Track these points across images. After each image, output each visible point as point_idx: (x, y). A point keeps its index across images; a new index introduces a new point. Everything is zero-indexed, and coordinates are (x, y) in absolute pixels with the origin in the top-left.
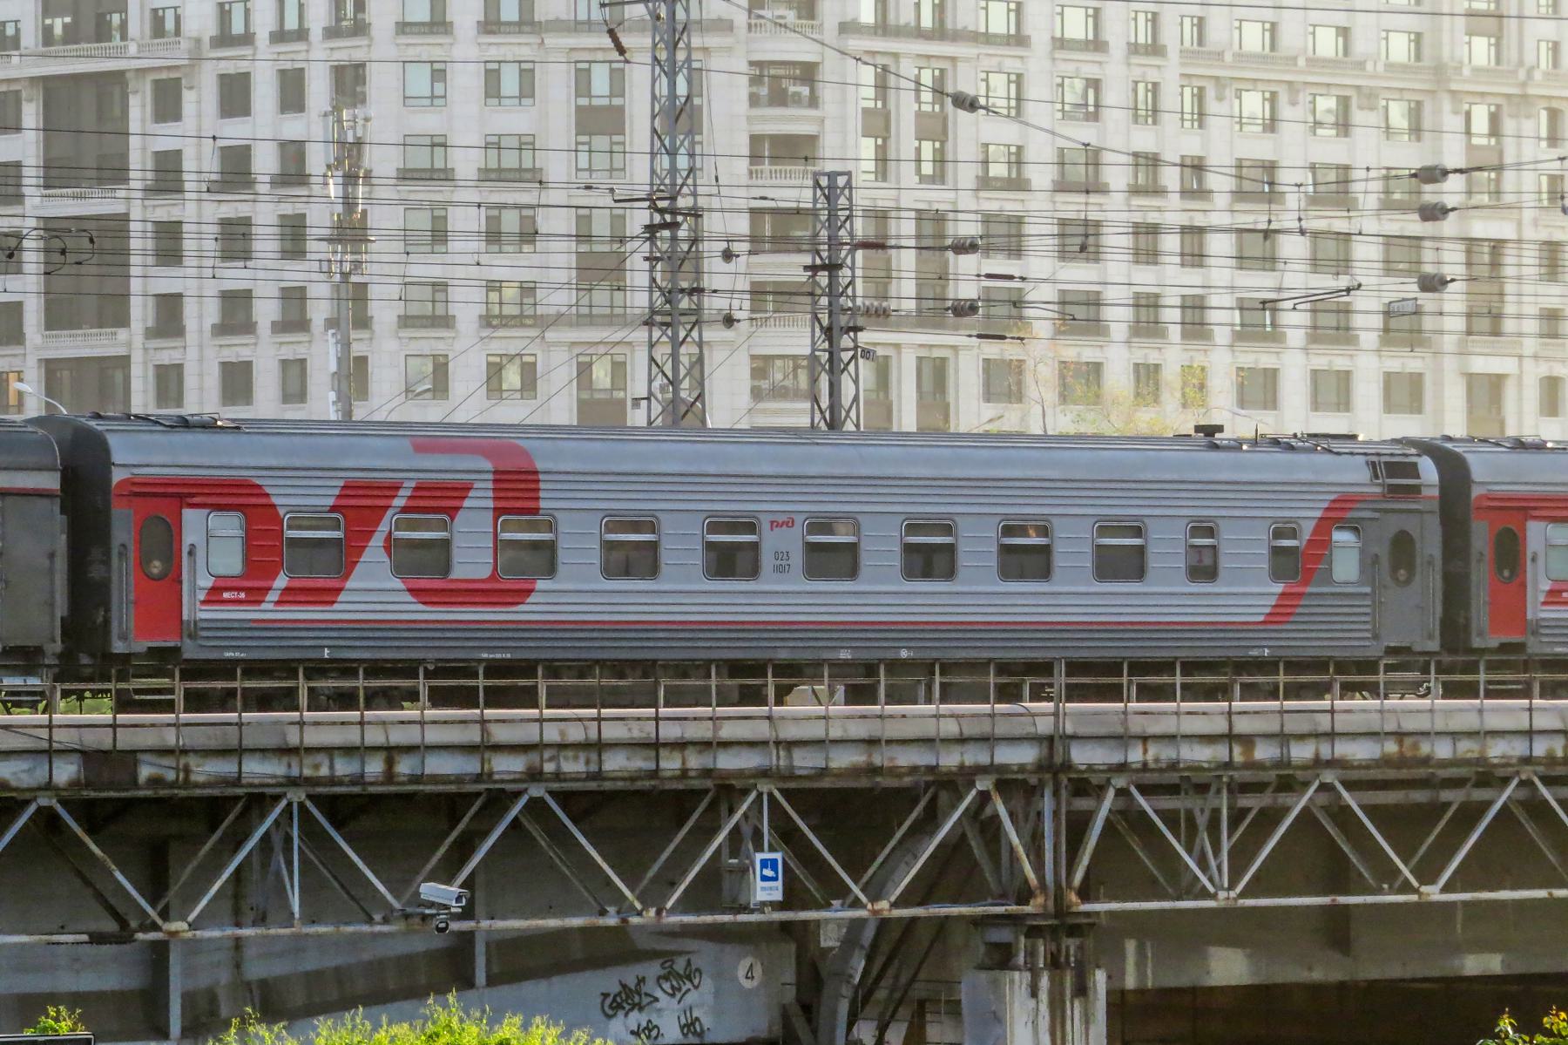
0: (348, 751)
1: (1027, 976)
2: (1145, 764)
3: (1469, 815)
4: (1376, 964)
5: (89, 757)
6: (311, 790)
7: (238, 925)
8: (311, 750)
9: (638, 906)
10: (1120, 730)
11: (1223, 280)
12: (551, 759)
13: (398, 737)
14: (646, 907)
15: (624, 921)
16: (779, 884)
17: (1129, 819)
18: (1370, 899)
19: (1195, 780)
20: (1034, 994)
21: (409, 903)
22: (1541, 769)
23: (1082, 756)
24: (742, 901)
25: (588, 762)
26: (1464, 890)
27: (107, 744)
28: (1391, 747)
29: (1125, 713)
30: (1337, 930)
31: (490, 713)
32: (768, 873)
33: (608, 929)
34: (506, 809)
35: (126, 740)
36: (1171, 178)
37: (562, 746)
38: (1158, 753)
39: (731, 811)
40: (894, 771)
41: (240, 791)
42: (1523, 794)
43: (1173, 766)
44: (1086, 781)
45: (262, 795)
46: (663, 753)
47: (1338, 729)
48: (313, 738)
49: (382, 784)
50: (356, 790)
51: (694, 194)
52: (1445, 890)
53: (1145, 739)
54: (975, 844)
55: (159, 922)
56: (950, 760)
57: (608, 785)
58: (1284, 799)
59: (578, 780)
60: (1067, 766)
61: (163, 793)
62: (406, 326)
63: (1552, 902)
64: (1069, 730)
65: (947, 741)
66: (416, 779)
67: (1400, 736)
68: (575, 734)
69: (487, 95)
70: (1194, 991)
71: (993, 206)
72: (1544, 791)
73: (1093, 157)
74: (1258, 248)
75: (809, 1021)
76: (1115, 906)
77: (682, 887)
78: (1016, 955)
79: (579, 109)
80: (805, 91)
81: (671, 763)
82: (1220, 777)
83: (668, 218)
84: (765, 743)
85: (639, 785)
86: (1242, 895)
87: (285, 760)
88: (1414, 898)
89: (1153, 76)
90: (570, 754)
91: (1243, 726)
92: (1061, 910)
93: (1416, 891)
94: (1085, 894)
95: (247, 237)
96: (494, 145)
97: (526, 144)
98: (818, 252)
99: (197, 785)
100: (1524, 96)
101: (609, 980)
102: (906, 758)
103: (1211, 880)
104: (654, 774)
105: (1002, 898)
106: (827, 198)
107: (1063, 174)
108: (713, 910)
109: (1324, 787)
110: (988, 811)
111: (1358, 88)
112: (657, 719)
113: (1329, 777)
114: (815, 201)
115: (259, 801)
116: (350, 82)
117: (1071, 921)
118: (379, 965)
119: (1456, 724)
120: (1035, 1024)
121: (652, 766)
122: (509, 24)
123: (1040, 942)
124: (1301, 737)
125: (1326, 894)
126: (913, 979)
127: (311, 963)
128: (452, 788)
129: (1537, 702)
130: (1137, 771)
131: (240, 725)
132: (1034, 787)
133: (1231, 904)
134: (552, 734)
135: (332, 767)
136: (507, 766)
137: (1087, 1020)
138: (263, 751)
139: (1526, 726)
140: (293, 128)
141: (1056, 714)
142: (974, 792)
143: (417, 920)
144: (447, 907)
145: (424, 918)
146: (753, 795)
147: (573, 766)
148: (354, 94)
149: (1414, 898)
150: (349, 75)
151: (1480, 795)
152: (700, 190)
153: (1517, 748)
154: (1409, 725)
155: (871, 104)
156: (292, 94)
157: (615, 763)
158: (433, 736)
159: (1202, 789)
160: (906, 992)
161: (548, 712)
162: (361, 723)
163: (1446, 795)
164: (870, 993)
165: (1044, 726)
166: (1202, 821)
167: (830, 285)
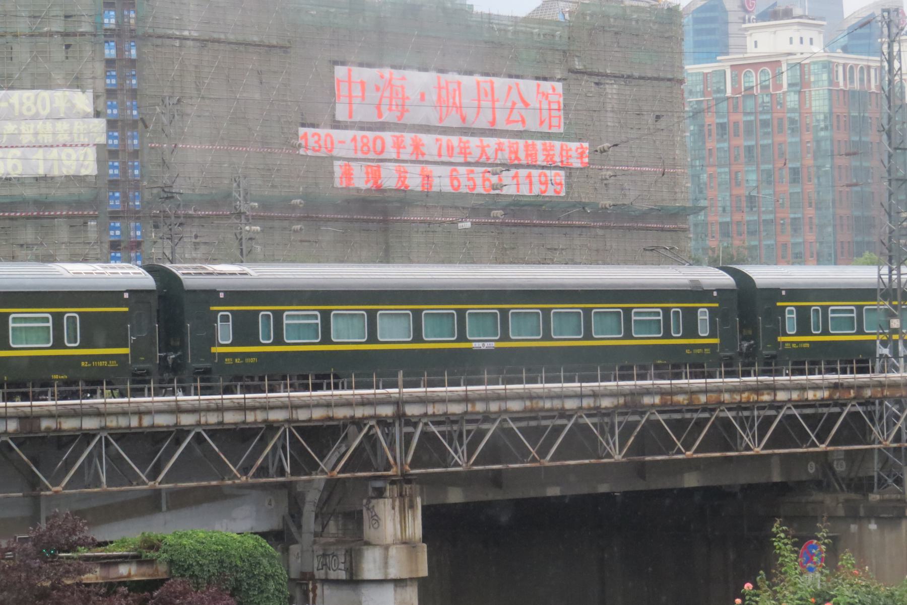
1: (391, 500)
3: (557, 430)
5: (24, 418)
8: (110, 414)
9: (239, 476)
19: (452, 418)
20: (393, 508)
23: (412, 410)
26: (559, 460)
30: (496, 479)
38: (439, 409)
43: (445, 414)
46: (248, 413)
50: (128, 431)
54: (368, 448)
55: (50, 487)
56: (359, 412)
57: (225, 427)
58: (485, 426)
60: (404, 415)
66: (153, 426)
70: (444, 506)
76: (423, 471)
81: (250, 417)
82: (462, 418)
86: (475, 464)
88: (537, 465)
90: (211, 414)
94: (413, 465)
99: (65, 431)
102: (341, 413)
104: (244, 422)
110: (371, 433)
115: (88, 436)
119: (552, 394)
120: (394, 520)
123: (396, 488)
130: (431, 416)
136: (187, 420)
137: (414, 520)
141: (399, 393)
147: (213, 419)
157: (230, 418)
163: (544, 423)
166: (455, 436)
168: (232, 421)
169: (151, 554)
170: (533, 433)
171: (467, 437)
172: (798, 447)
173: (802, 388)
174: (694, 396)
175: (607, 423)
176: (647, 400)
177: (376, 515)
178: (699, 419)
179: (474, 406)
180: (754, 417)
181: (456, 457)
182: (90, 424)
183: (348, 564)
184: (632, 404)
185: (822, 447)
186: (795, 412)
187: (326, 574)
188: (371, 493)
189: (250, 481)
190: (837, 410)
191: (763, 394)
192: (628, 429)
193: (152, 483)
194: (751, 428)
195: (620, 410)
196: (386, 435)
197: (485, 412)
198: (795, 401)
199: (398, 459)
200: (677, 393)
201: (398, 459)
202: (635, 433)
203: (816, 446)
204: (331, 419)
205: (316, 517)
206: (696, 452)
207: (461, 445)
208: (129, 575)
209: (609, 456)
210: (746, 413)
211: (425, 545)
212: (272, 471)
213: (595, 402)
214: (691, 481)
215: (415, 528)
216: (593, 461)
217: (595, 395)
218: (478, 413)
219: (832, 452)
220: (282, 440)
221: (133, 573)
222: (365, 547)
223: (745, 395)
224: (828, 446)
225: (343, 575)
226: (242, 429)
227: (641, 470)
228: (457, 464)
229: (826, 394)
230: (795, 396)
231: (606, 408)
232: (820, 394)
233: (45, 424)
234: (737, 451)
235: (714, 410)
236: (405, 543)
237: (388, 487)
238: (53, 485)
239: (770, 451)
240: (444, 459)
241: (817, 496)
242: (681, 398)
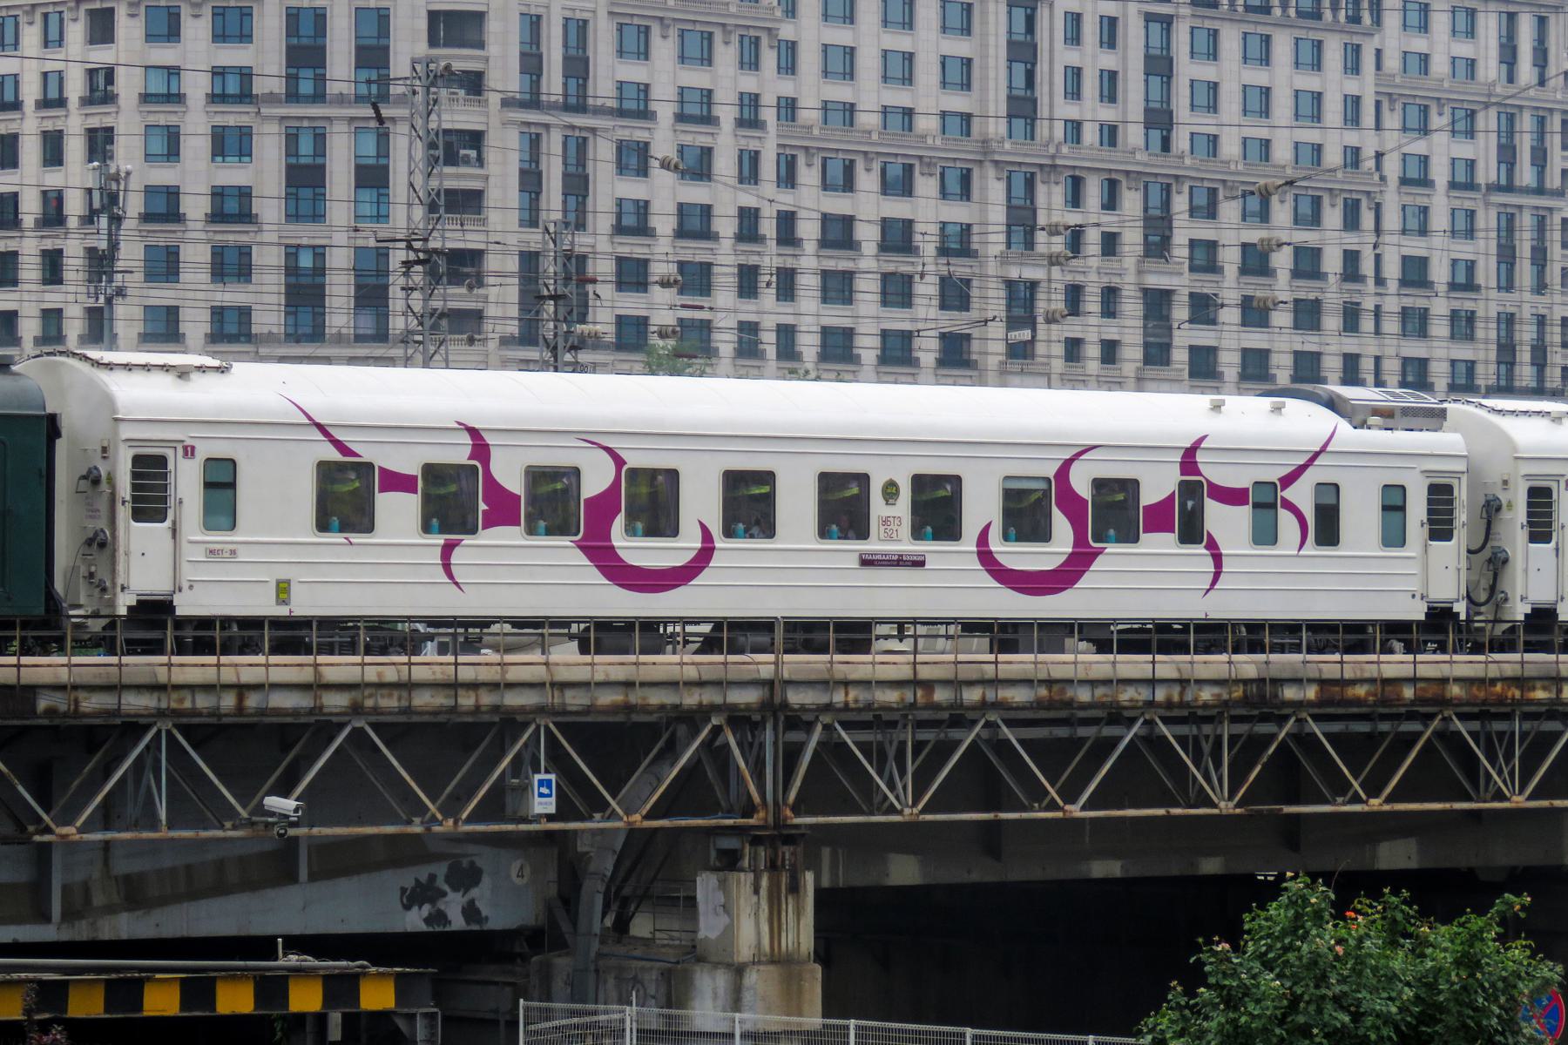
0: (208, 688)
1: (751, 876)
2: (846, 704)
4: (1020, 870)
6: (176, 721)
7: (107, 828)
9: (439, 817)
10: (826, 676)
11: (811, 313)
12: (370, 696)
13: (248, 676)
14: (446, 817)
15: (428, 829)
16: (553, 799)
17: (833, 750)
18: (1025, 815)
19: (886, 716)
20: (756, 891)
21: (251, 814)
23: (795, 698)
24: (522, 813)
25: (399, 699)
27: (12, 680)
28: (1043, 692)
29: (831, 662)
30: (991, 839)
31: (322, 659)
32: (545, 790)
33: (417, 836)
34: (331, 739)
35: (28, 677)
36: (768, 228)
37: (381, 685)
39: (515, 740)
40: (645, 709)
41: (118, 721)
42: (1143, 732)
43: (869, 707)
45: (136, 723)
46: (461, 692)
47: (1001, 676)
48: (179, 677)
49: (235, 715)
51: (443, 237)
52: (1083, 808)
53: (847, 684)
55: (53, 826)
56: (691, 699)
57: (415, 719)
58: (955, 734)
59: (390, 713)
60: (785, 705)
61: (57, 722)
62: (145, 341)
63: (1169, 817)
64: (786, 676)
65: (690, 684)
66: (262, 712)
67: (1049, 683)
68: (390, 675)
69: (214, 155)
71: (624, 251)
72: (1164, 729)
73: (706, 211)
74: (838, 287)
75: (568, 911)
76: (821, 819)
77: (475, 802)
78: (742, 857)
79: (290, 168)
80: (473, 154)
81: (467, 700)
83: (421, 256)
84: (542, 685)
85: (441, 719)
87: (156, 695)
88: (1059, 814)
89: (753, 145)
90: (385, 691)
91: (925, 673)
92: (779, 823)
93: (1062, 809)
94: (797, 809)
95: (16, 269)
96: (218, 194)
97: (245, 194)
98: (546, 285)
99: (86, 715)
100: (1054, 166)
101: (408, 877)
102: (656, 698)
103: (897, 798)
104: (454, 710)
105: (729, 813)
106: (554, 242)
107: (681, 224)
108: (503, 819)
109: (988, 725)
110: (717, 743)
111: (920, 157)
112: (456, 664)
113: (993, 717)
114: (545, 243)
115: (133, 728)
116: (100, 143)
117: (785, 832)
118: (220, 865)
120: (756, 915)
121: (451, 702)
122: (233, 96)
123: (762, 852)
124: (971, 683)
125: (987, 811)
126: (655, 878)
127: (167, 862)
128: (289, 720)
129: (1159, 657)
130: (839, 710)
131: (120, 665)
132: (757, 723)
133: (913, 818)
134: (371, 675)
135: (193, 701)
136: (336, 702)
138: (139, 688)
139: (1150, 676)
140: (54, 179)
141: (776, 663)
143: (261, 827)
144: (287, 817)
145: (267, 825)
146: (533, 727)
147: (390, 702)
148: (104, 152)
150: (99, 134)
151: (1108, 731)
152: (448, 235)
153: (1143, 694)
154: (1058, 673)
155: (526, 166)
156: (53, 151)
157: (422, 700)
158: (277, 675)
159: (893, 724)
160: (648, 889)
161: (368, 659)
162: (218, 665)
163: (1082, 732)
164: (619, 889)
165: (766, 672)
166: (891, 752)
167: (556, 312)
171: (916, 754)
174: (1388, 689)
175: (1207, 737)
176: (1290, 693)
178: (1398, 735)
180: (1513, 733)
181: (891, 797)
182: (135, 703)
184: (1260, 700)
191: (1534, 689)
192: (1249, 749)
194: (1509, 756)
197: (951, 707)
201: (765, 791)
202: (1265, 759)
207: (902, 773)
210: (1498, 726)
211: (818, 969)
213: (1182, 694)
214: (1396, 855)
215: (801, 933)
218: (937, 707)
222: (697, 968)
223: (1499, 688)
227: (1292, 833)
228: (892, 810)
231: (1205, 706)
236: (772, 962)
237: (747, 850)
239: (1545, 803)
240: (870, 799)
242: (1361, 691)
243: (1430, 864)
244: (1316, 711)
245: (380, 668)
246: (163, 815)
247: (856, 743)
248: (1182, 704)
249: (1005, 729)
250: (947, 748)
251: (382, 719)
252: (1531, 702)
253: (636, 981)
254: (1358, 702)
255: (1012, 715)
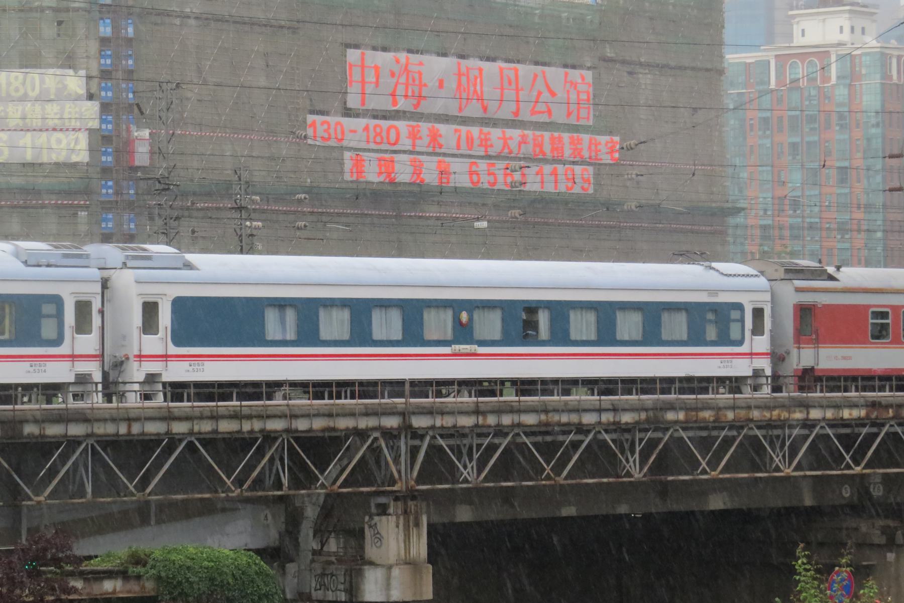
1: (394, 517)
9: (233, 488)
14: (236, 488)
17: (435, 450)
20: (397, 527)
22: (604, 427)
23: (419, 422)
28: (543, 417)
30: (507, 496)
38: (448, 421)
39: (270, 448)
44: (416, 432)
52: (566, 478)
55: (32, 496)
56: (363, 423)
60: (410, 426)
66: (143, 434)
81: (246, 426)
87: (86, 425)
88: (553, 482)
90: (205, 422)
102: (343, 423)
103: (468, 473)
110: (375, 445)
113: (516, 431)
115: (74, 443)
123: (400, 504)
132: (395, 437)
135: (105, 428)
136: (179, 428)
139: (598, 407)
141: (406, 403)
142: (372, 438)
147: (206, 427)
149: (553, 482)
157: (226, 426)
159: (464, 436)
166: (465, 451)
168: (227, 430)
169: (140, 569)
170: (548, 450)
172: (833, 469)
173: (837, 407)
175: (627, 440)
176: (670, 416)
177: (378, 533)
179: (485, 418)
182: (76, 430)
183: (347, 585)
185: (858, 469)
186: (830, 432)
187: (325, 596)
188: (373, 510)
189: (246, 494)
190: (875, 430)
191: (795, 412)
193: (139, 495)
195: (642, 426)
196: (391, 448)
197: (498, 425)
198: (829, 420)
199: (404, 473)
200: (702, 409)
202: (657, 451)
203: (853, 469)
204: (334, 429)
205: (314, 536)
206: (721, 472)
207: (471, 460)
208: (114, 592)
209: (628, 474)
211: (430, 566)
212: (269, 482)
213: (614, 417)
214: (717, 503)
215: (420, 548)
216: (611, 480)
217: (615, 409)
218: (490, 426)
219: (869, 475)
220: (280, 449)
221: (118, 589)
222: (366, 567)
223: (775, 413)
224: (864, 468)
225: (343, 597)
226: (236, 439)
227: (664, 490)
229: (863, 413)
230: (829, 414)
231: (627, 424)
232: (855, 413)
233: (29, 429)
234: (767, 472)
235: (742, 427)
238: (37, 495)
240: (452, 474)
241: (851, 523)
242: (707, 415)
243: (729, 506)
244: (684, 425)
245: (201, 409)
246: (89, 489)
247: (447, 446)
248: (614, 423)
249: (524, 437)
250: (492, 448)
251: (201, 436)
252: (793, 420)
253: (332, 575)
254: (704, 420)
255: (528, 430)
